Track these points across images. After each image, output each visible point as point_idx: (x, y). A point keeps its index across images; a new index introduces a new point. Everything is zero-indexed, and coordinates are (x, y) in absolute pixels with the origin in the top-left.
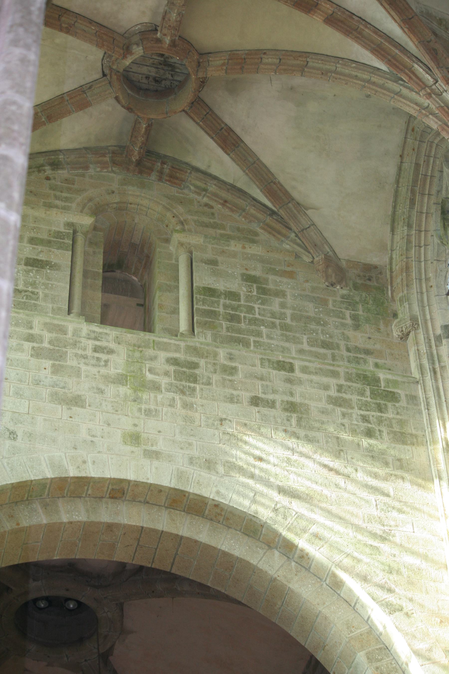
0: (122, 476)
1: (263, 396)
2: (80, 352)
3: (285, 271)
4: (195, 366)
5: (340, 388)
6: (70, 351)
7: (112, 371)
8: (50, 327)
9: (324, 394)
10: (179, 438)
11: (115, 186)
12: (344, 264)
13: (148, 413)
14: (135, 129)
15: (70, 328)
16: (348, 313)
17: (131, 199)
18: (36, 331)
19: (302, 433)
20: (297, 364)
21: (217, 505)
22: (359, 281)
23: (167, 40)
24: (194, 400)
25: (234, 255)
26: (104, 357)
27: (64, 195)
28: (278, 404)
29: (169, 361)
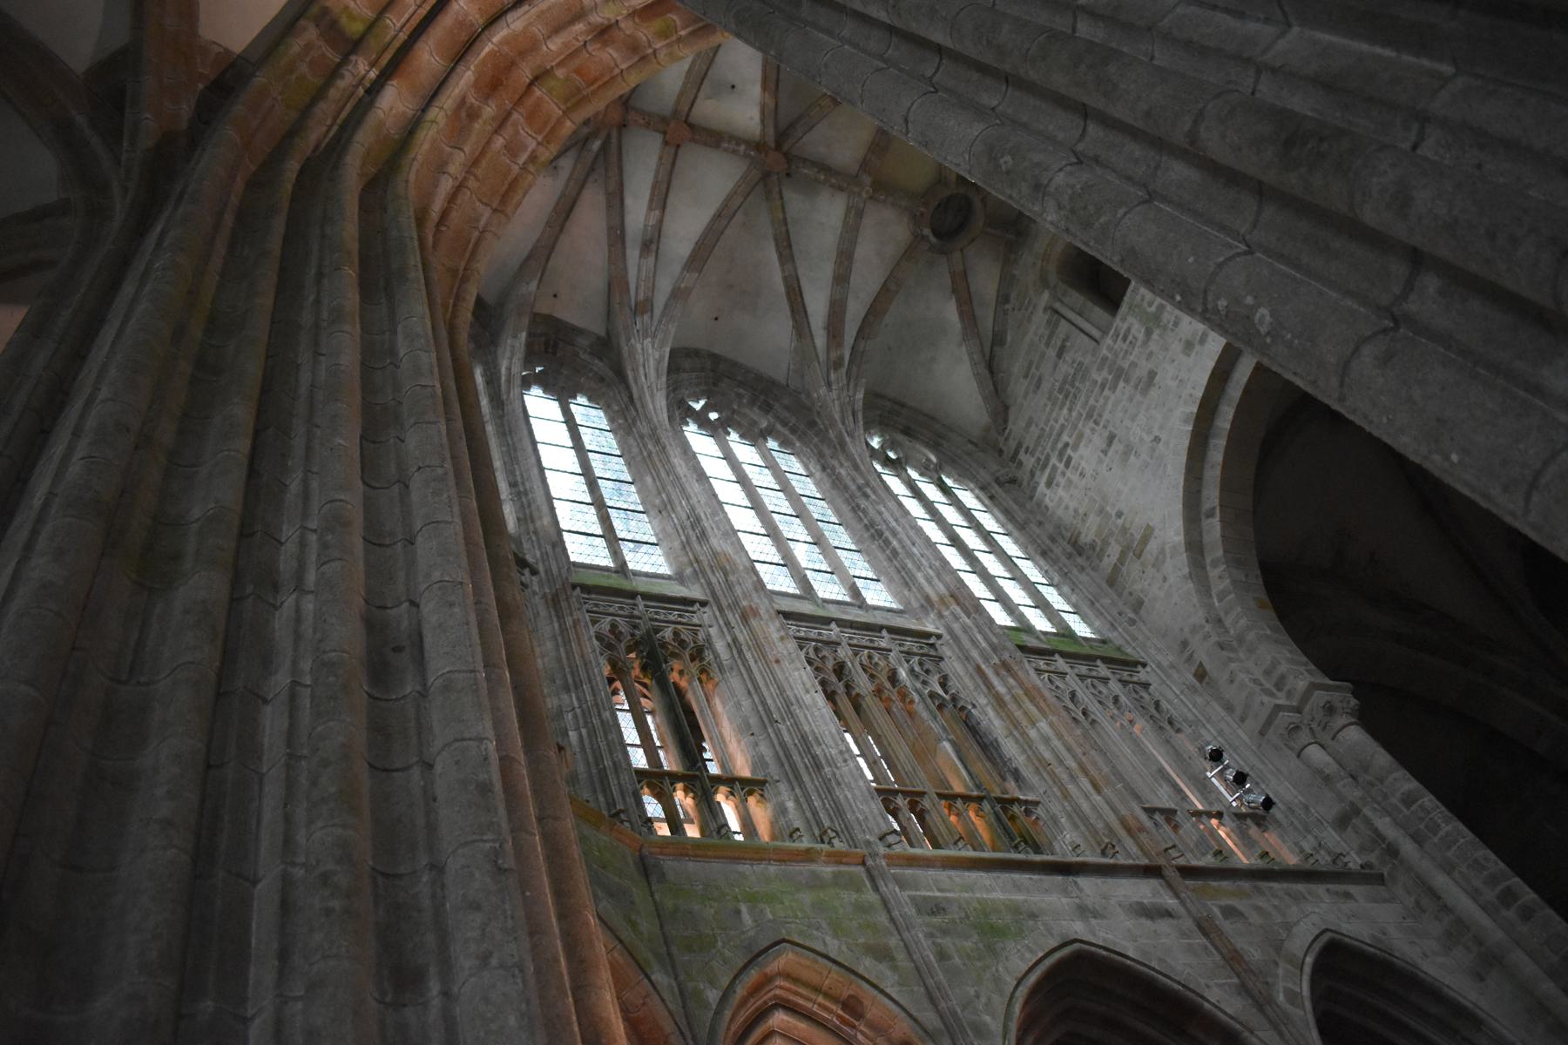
0: (1209, 372)
2: (1122, 354)
7: (1141, 336)
8: (1100, 369)
23: (922, 209)
26: (1130, 338)
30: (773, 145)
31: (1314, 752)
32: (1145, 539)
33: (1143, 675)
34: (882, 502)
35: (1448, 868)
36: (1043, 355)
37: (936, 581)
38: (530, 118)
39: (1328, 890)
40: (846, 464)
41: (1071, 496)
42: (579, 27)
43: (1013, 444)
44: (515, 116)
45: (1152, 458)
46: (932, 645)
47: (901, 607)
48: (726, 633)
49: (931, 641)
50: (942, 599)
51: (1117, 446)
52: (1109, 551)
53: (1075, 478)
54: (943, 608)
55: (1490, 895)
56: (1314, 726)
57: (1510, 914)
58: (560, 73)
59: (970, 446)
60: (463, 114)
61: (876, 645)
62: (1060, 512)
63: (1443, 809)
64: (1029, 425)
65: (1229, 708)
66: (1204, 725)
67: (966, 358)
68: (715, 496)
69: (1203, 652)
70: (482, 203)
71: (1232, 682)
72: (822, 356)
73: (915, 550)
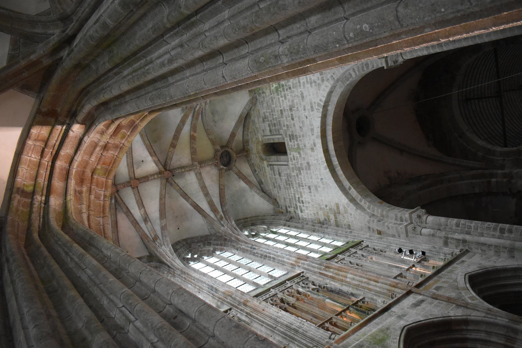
0: (322, 152)
1: (291, 117)
2: (296, 163)
3: (258, 112)
4: (289, 135)
5: (282, 97)
6: (297, 166)
7: (298, 155)
8: (293, 172)
9: (284, 101)
10: (308, 138)
11: (255, 156)
12: (251, 97)
13: (305, 146)
14: (240, 156)
15: (291, 166)
16: (263, 95)
17: (256, 151)
18: (295, 174)
19: (296, 106)
20: (280, 109)
21: (321, 127)
22: (254, 93)
23: (216, 161)
24: (298, 135)
25: (259, 125)
27: (261, 168)
28: (292, 113)
29: (291, 142)
30: (164, 170)
31: (424, 231)
32: (338, 207)
33: (364, 244)
34: (260, 247)
35: (482, 235)
36: (275, 179)
37: (291, 258)
38: (97, 186)
39: (457, 264)
40: (243, 244)
41: (310, 210)
42: (98, 149)
43: (284, 208)
44: (93, 187)
45: (324, 185)
46: (303, 276)
47: (286, 272)
48: (243, 313)
49: (302, 275)
50: (296, 262)
51: (313, 188)
52: (331, 218)
53: (307, 205)
54: (298, 264)
55: (498, 233)
56: (419, 224)
57: (506, 234)
58: (99, 167)
59: (273, 217)
60: (78, 194)
61: (287, 287)
62: (310, 217)
63: (468, 220)
64: (285, 199)
65: (394, 236)
66: (391, 245)
67: (255, 194)
68: (212, 277)
69: (375, 226)
70: (98, 217)
71: (389, 228)
72: (216, 219)
73: (279, 254)
